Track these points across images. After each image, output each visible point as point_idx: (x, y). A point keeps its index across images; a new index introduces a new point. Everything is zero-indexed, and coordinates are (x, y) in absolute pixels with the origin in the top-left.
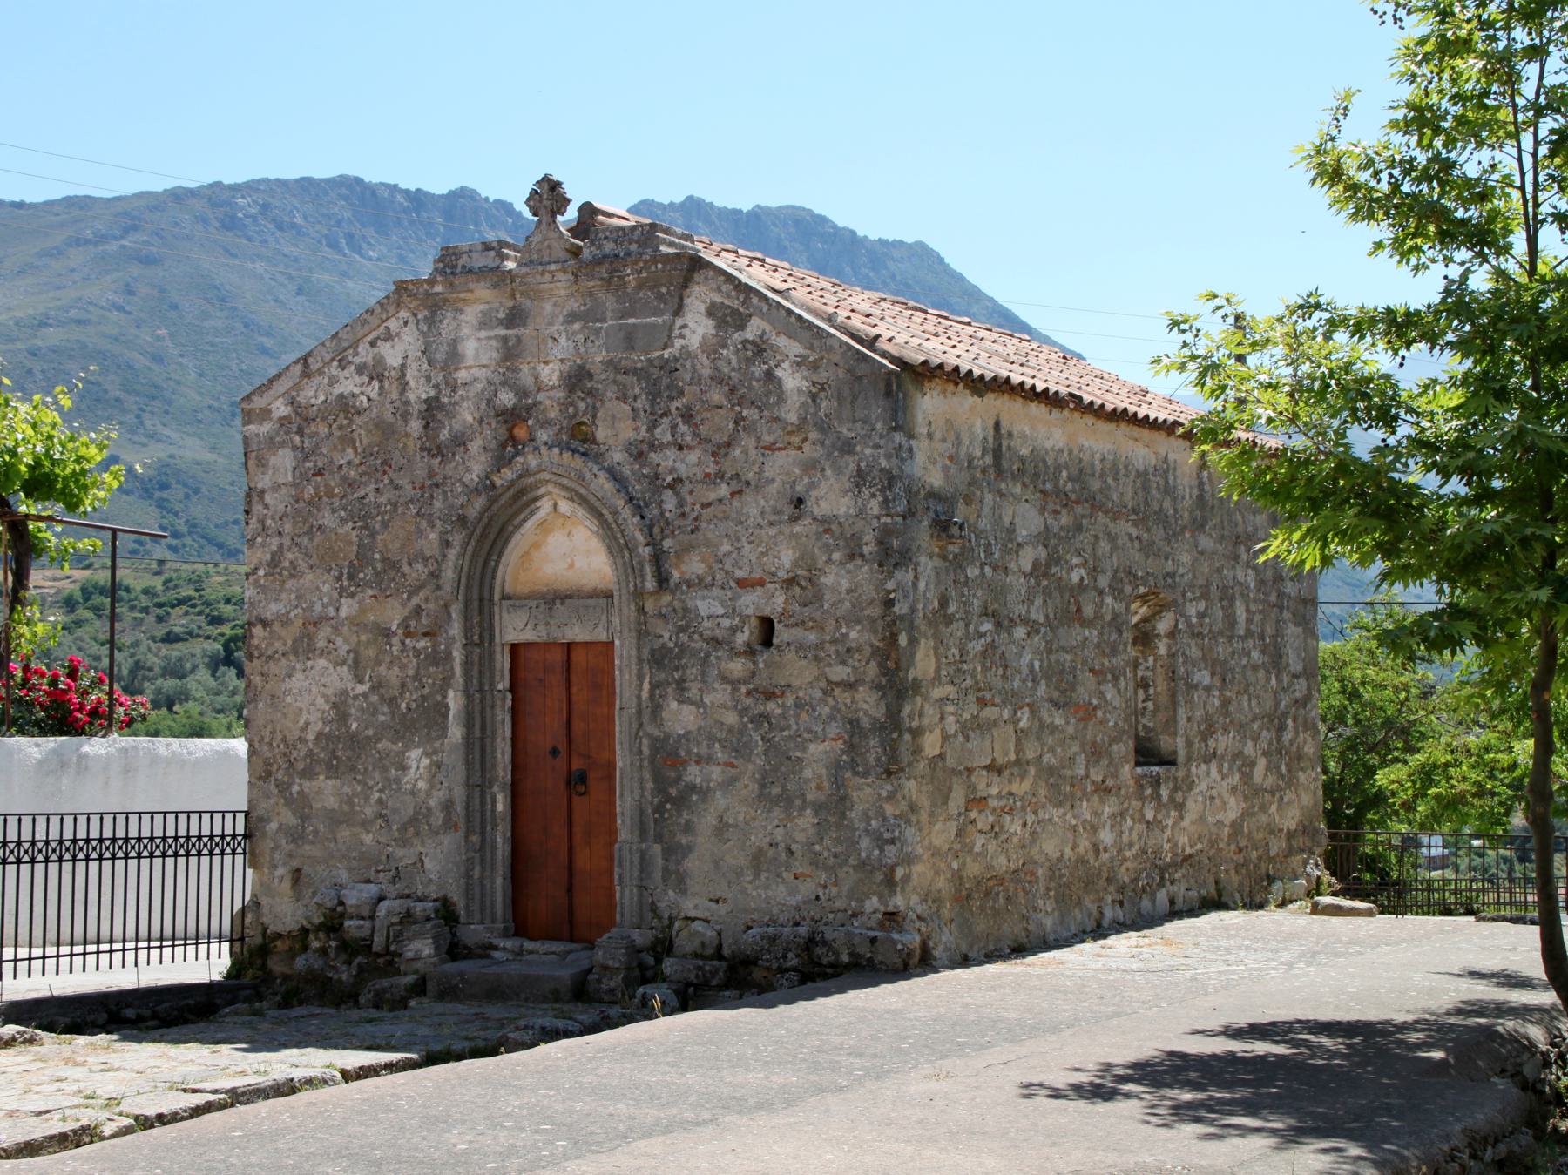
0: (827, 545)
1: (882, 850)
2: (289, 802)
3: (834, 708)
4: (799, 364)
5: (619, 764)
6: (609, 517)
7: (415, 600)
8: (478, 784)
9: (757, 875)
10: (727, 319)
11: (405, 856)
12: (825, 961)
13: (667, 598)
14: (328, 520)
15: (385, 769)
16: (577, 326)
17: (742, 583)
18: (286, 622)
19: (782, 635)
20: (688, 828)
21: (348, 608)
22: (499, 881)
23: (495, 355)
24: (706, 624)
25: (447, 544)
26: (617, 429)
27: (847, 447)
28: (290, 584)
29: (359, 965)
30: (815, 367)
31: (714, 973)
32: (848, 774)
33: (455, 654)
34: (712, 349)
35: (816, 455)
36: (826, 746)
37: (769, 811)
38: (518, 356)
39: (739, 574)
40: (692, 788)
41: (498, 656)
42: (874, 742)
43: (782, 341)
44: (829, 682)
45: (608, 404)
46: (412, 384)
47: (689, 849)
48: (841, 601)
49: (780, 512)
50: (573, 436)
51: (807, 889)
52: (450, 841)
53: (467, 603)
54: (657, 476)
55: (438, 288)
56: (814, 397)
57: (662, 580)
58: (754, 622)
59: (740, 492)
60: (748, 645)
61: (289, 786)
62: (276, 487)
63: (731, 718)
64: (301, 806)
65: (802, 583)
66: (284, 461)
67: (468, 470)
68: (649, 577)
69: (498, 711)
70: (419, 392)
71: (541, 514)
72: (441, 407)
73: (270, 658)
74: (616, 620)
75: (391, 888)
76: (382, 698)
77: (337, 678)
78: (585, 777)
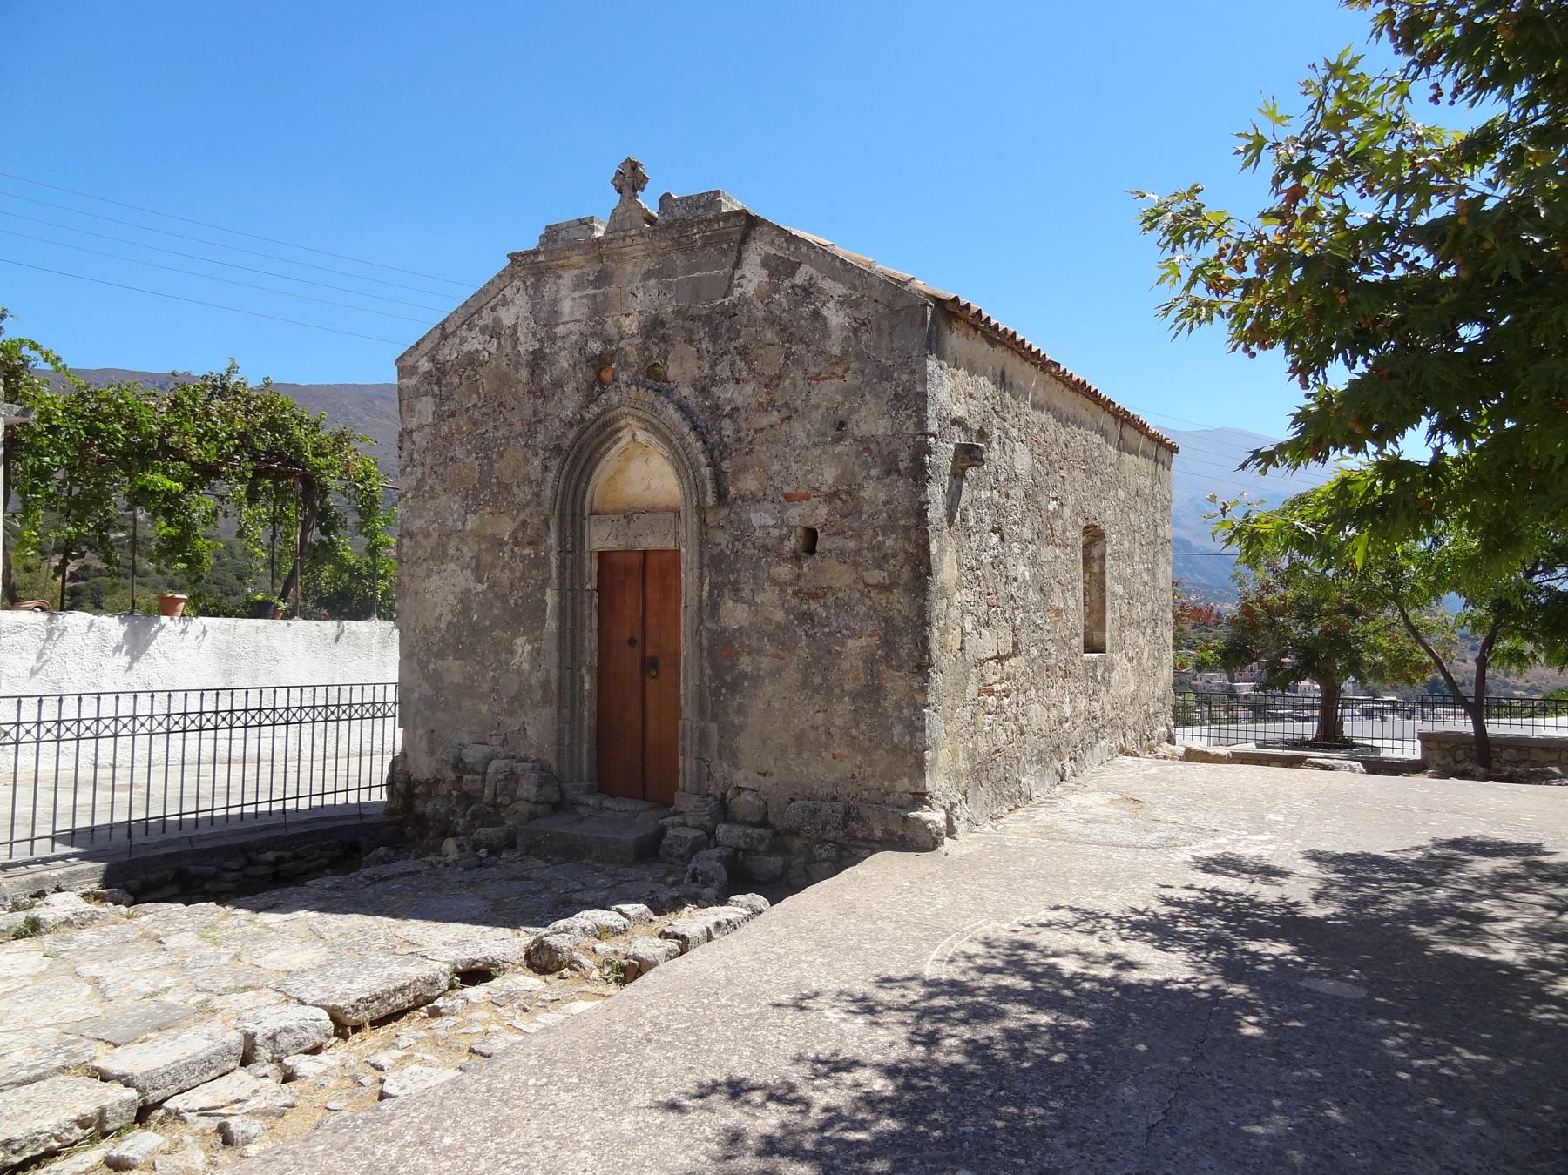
0: (866, 462)
1: (913, 736)
2: (426, 678)
3: (869, 608)
4: (842, 303)
5: (684, 653)
6: (676, 442)
7: (522, 516)
9: (800, 753)
10: (779, 268)
11: (512, 724)
12: (859, 835)
13: (724, 512)
14: (459, 452)
15: (498, 653)
16: (652, 282)
19: (824, 542)
20: (741, 710)
21: (472, 522)
22: (585, 748)
23: (586, 310)
24: (757, 533)
25: (546, 469)
26: (682, 368)
27: (885, 375)
28: (430, 504)
29: (473, 813)
30: (856, 305)
31: (761, 839)
32: (883, 668)
33: (553, 559)
34: (766, 295)
35: (857, 382)
36: (863, 641)
37: (811, 698)
38: (605, 311)
39: (787, 489)
40: (745, 676)
41: (587, 562)
42: (907, 639)
43: (827, 284)
44: (866, 585)
45: (678, 347)
46: (522, 340)
47: (741, 728)
48: (878, 512)
49: (824, 435)
50: (648, 377)
51: (845, 767)
52: (548, 713)
54: (717, 407)
55: (542, 258)
56: (855, 331)
57: (721, 496)
58: (800, 532)
59: (789, 418)
60: (794, 552)
61: (428, 663)
62: (421, 428)
63: (779, 616)
64: (436, 679)
65: (843, 497)
66: (426, 406)
67: (564, 408)
68: (709, 493)
69: (586, 606)
70: (527, 345)
71: (623, 442)
72: (544, 357)
73: (415, 562)
74: (682, 531)
75: (501, 750)
76: (497, 596)
78: (656, 666)
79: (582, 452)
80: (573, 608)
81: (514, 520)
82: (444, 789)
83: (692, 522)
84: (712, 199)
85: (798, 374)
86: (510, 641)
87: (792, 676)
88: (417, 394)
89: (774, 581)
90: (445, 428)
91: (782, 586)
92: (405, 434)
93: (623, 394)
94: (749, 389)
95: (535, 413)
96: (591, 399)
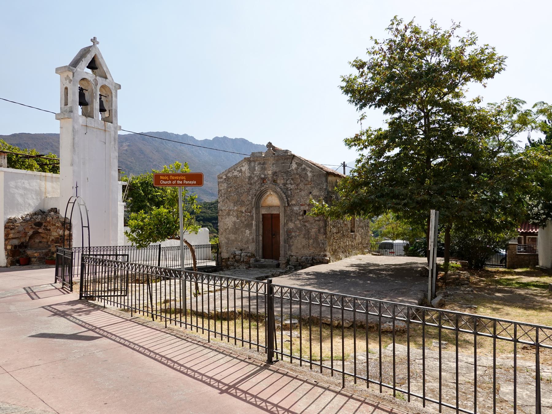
8: (257, 236)
17: (301, 205)
18: (225, 210)
20: (292, 242)
21: (236, 208)
26: (280, 182)
34: (297, 169)
43: (308, 168)
51: (312, 251)
57: (288, 204)
63: (299, 225)
64: (228, 239)
66: (225, 185)
70: (248, 174)
77: (234, 219)
79: (260, 196)
82: (231, 259)
83: (283, 209)
84: (287, 151)
85: (303, 183)
87: (302, 236)
88: (222, 182)
89: (298, 219)
90: (229, 190)
91: (300, 220)
92: (220, 191)
93: (268, 184)
96: (262, 186)
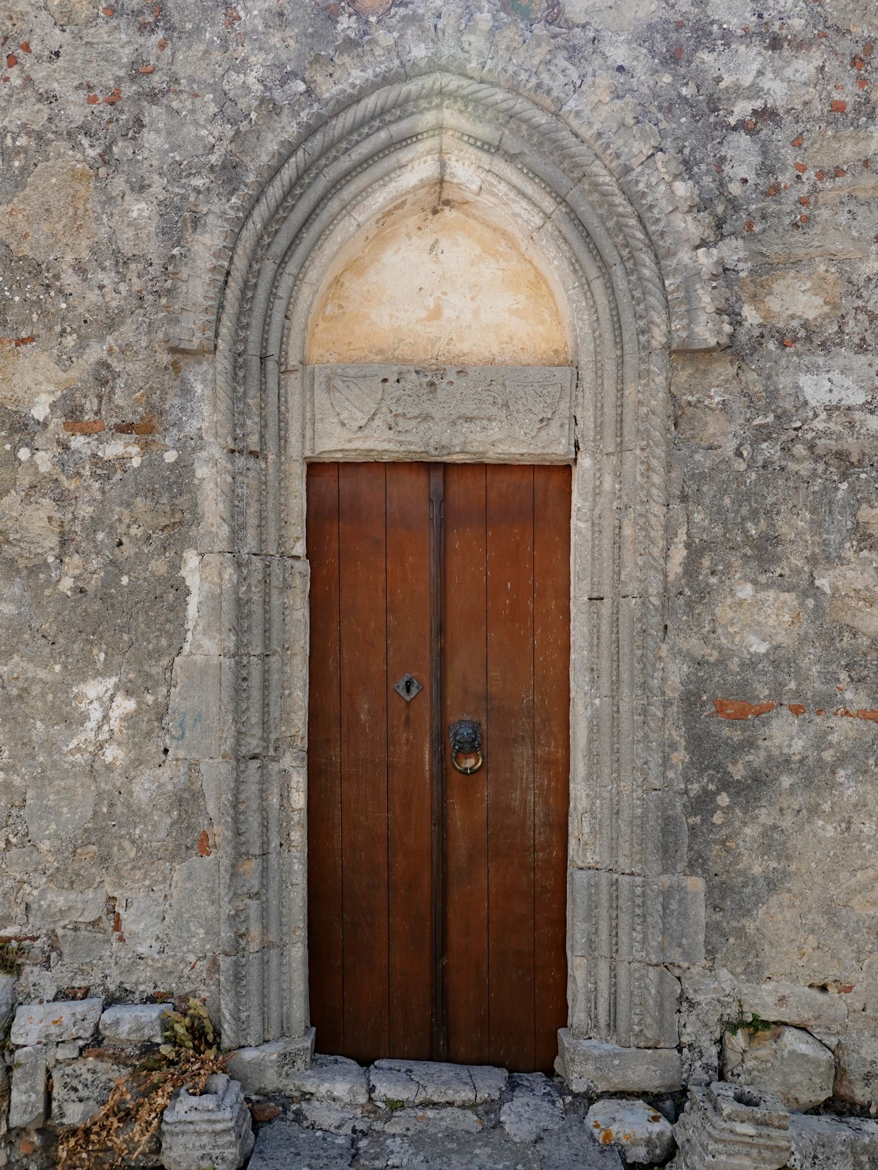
53: (238, 361)
80: (266, 602)
81: (65, 361)
86: (63, 687)
94: (804, 67)
95: (139, 70)
